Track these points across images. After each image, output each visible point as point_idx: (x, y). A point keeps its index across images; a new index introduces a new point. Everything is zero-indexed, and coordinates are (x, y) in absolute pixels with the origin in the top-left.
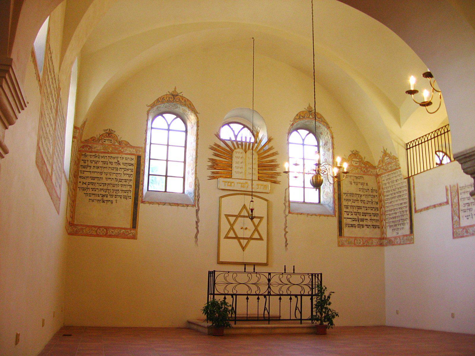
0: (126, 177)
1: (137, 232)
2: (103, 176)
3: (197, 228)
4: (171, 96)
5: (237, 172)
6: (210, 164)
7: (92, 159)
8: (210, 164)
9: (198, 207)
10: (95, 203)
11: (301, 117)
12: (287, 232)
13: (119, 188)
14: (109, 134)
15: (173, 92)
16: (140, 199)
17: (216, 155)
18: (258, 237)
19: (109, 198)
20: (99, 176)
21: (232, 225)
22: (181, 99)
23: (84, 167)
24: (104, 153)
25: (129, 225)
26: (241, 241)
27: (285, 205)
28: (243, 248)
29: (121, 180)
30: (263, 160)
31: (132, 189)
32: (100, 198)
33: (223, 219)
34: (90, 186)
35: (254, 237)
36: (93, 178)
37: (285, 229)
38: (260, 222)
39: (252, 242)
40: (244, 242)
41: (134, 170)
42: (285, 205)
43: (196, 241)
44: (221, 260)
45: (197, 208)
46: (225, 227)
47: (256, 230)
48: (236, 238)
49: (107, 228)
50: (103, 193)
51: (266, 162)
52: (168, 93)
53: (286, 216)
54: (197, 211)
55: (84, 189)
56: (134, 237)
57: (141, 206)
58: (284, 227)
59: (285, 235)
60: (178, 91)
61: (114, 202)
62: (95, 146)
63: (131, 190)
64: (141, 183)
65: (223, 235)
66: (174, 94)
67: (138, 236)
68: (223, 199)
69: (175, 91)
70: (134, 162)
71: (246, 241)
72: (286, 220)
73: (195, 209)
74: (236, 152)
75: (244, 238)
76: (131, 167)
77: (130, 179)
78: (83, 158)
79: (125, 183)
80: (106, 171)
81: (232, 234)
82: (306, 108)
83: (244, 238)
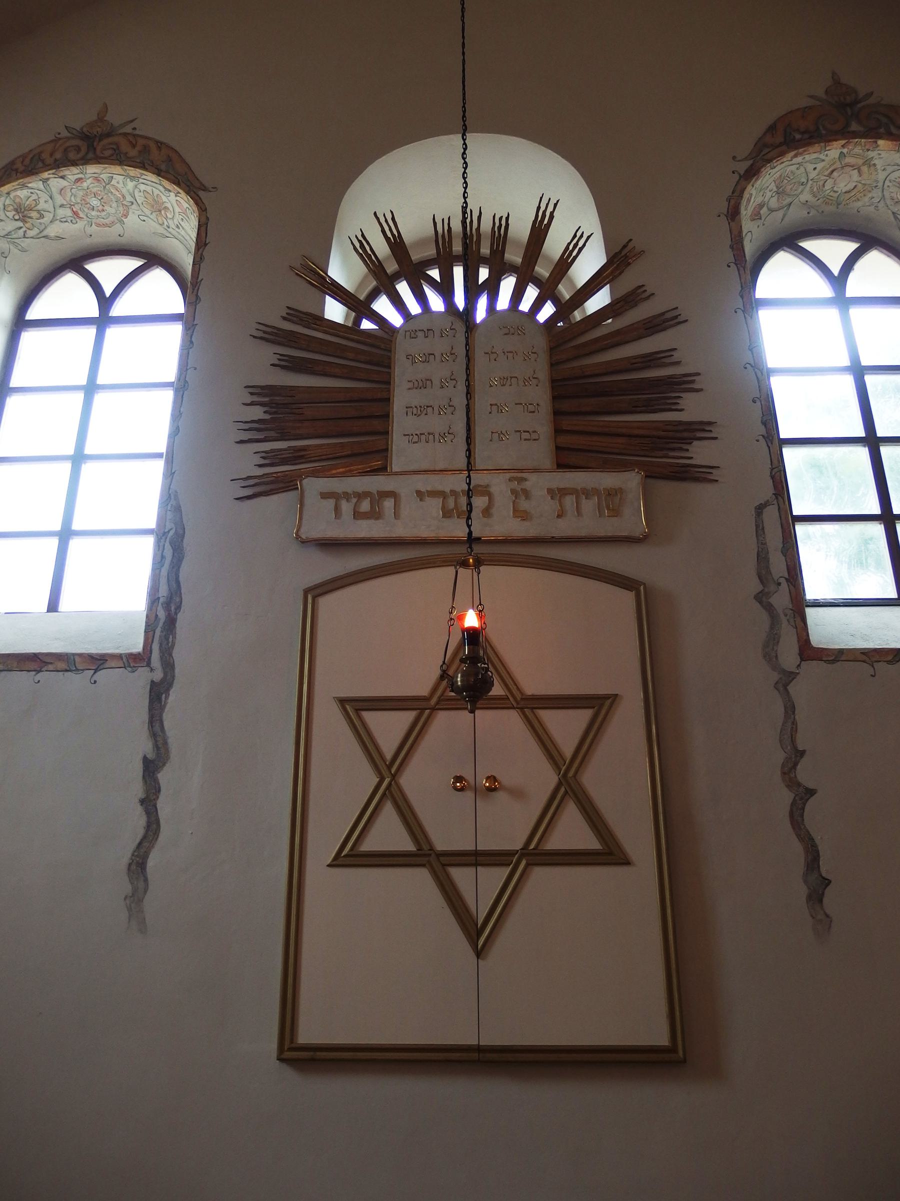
3: (149, 803)
5: (416, 438)
9: (168, 665)
11: (798, 136)
12: (811, 792)
18: (592, 843)
21: (389, 770)
22: (125, 147)
26: (461, 876)
27: (769, 608)
28: (478, 934)
33: (329, 722)
35: (555, 842)
37: (789, 771)
39: (542, 877)
40: (480, 887)
42: (769, 608)
44: (305, 1036)
45: (158, 675)
46: (343, 782)
47: (569, 788)
48: (424, 856)
52: (65, 133)
53: (786, 679)
54: (158, 694)
58: (780, 757)
60: (114, 118)
65: (324, 842)
68: (327, 603)
71: (493, 878)
72: (790, 709)
73: (141, 679)
75: (477, 858)
81: (388, 834)
82: (824, 96)
83: (477, 858)
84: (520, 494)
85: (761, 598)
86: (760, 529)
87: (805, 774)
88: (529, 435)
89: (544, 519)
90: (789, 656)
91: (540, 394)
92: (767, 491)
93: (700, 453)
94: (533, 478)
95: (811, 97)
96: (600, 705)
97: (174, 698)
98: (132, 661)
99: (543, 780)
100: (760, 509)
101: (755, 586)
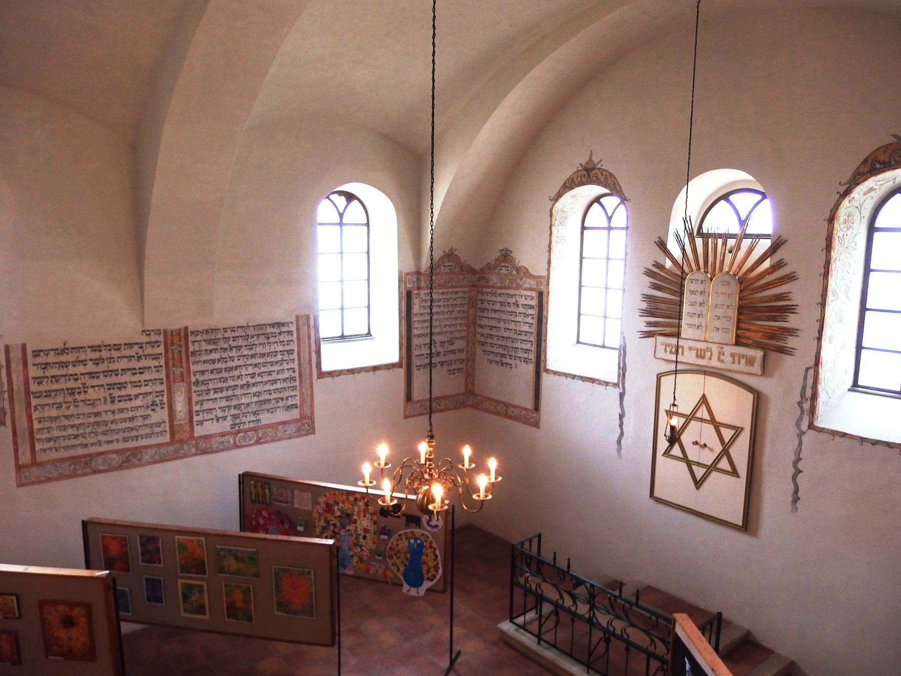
0: (526, 328)
1: (539, 418)
2: (502, 325)
3: (621, 425)
4: (583, 172)
5: (690, 326)
6: (644, 305)
7: (490, 298)
8: (644, 305)
9: (624, 389)
10: (494, 366)
11: (878, 166)
12: (801, 472)
13: (518, 345)
14: (506, 256)
15: (587, 163)
16: (542, 364)
17: (656, 287)
19: (508, 360)
20: (497, 324)
22: (600, 176)
23: (482, 310)
24: (501, 288)
25: (530, 406)
27: (802, 408)
28: (698, 484)
29: (520, 333)
30: (756, 296)
31: (534, 348)
32: (498, 359)
34: (489, 340)
36: (492, 328)
37: (795, 464)
38: (734, 438)
41: (536, 317)
42: (802, 408)
43: (619, 450)
47: (725, 452)
49: (507, 405)
50: (500, 351)
51: (763, 300)
53: (801, 434)
54: (622, 396)
55: (483, 344)
56: (536, 425)
57: (545, 377)
58: (793, 458)
59: (794, 477)
60: (595, 159)
61: (514, 366)
62: (491, 277)
63: (532, 349)
64: (543, 338)
66: (591, 166)
67: (542, 424)
69: (591, 160)
70: (534, 303)
72: (800, 444)
73: (617, 391)
74: (692, 281)
76: (531, 312)
77: (531, 330)
78: (480, 297)
79: (524, 338)
80: (504, 316)
84: (721, 353)
85: (800, 404)
86: (806, 377)
87: (800, 466)
88: (725, 330)
89: (727, 364)
90: (804, 426)
91: (733, 313)
92: (812, 362)
93: (791, 342)
94: (726, 347)
95: (894, 136)
96: (738, 430)
97: (626, 398)
98: (616, 385)
99: (719, 448)
100: (807, 369)
101: (798, 398)
